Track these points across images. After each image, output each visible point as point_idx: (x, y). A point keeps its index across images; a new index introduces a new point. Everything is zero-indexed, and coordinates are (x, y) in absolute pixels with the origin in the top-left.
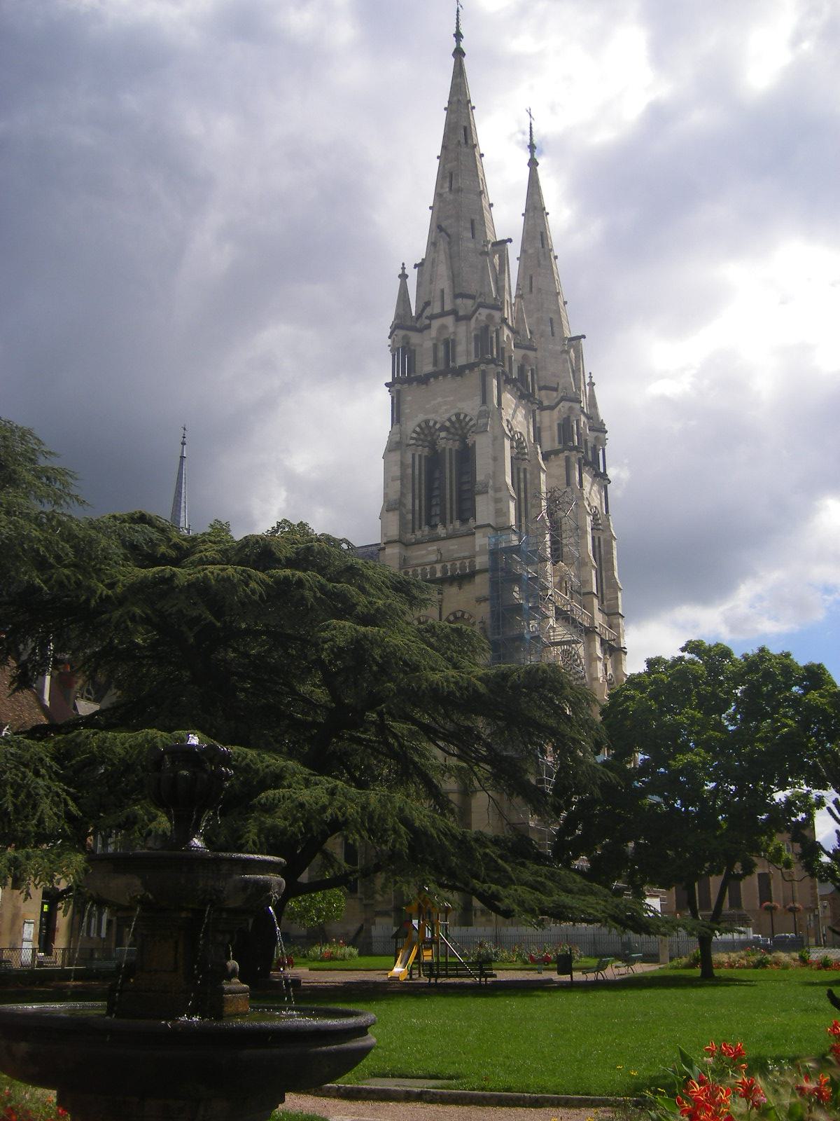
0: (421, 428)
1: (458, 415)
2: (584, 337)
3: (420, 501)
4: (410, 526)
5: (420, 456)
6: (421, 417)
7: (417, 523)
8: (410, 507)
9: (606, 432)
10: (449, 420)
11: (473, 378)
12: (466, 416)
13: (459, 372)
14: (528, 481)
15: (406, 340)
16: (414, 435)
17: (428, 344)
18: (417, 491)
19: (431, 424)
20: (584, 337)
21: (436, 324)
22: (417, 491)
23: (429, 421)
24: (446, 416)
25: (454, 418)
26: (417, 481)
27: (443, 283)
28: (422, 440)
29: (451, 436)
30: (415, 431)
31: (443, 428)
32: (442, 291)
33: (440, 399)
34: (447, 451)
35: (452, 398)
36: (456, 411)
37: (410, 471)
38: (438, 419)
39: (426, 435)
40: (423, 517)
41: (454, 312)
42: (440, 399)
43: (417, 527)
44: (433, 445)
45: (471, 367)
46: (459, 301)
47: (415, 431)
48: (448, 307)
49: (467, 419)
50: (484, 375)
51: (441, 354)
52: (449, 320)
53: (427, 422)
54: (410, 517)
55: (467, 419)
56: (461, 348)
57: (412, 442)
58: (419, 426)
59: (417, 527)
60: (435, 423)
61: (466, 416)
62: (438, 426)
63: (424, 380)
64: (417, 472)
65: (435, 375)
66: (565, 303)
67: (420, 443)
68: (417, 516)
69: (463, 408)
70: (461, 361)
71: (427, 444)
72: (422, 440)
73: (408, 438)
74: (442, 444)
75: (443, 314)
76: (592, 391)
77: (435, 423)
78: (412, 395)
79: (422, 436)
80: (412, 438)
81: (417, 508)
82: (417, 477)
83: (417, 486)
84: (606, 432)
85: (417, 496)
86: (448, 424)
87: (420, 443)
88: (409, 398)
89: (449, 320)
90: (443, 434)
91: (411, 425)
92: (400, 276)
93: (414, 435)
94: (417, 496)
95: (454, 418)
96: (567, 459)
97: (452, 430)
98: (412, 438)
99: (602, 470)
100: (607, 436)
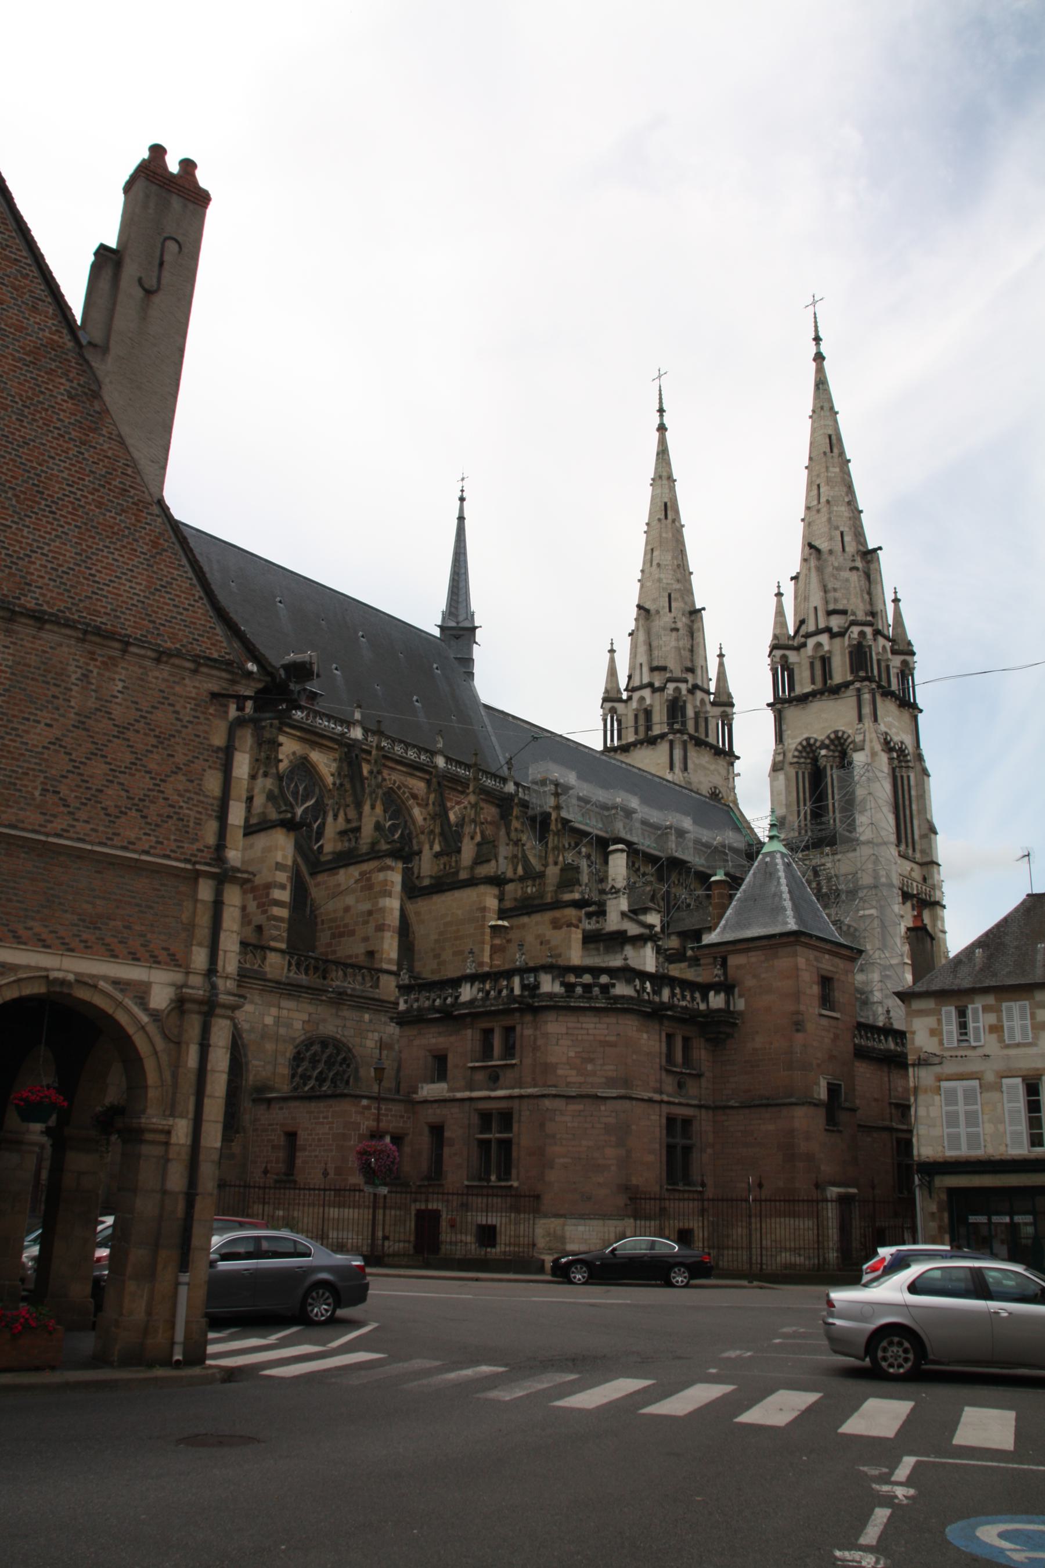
13: (835, 691)
15: (784, 657)
19: (812, 741)
21: (811, 642)
27: (816, 599)
29: (831, 753)
31: (823, 746)
32: (816, 608)
48: (821, 625)
51: (818, 672)
52: (824, 638)
62: (818, 744)
63: (804, 699)
65: (813, 694)
67: (802, 760)
75: (818, 632)
78: (792, 713)
79: (804, 754)
86: (827, 742)
87: (802, 760)
89: (824, 638)
90: (823, 752)
91: (792, 743)
92: (776, 595)
97: (832, 747)
98: (794, 757)
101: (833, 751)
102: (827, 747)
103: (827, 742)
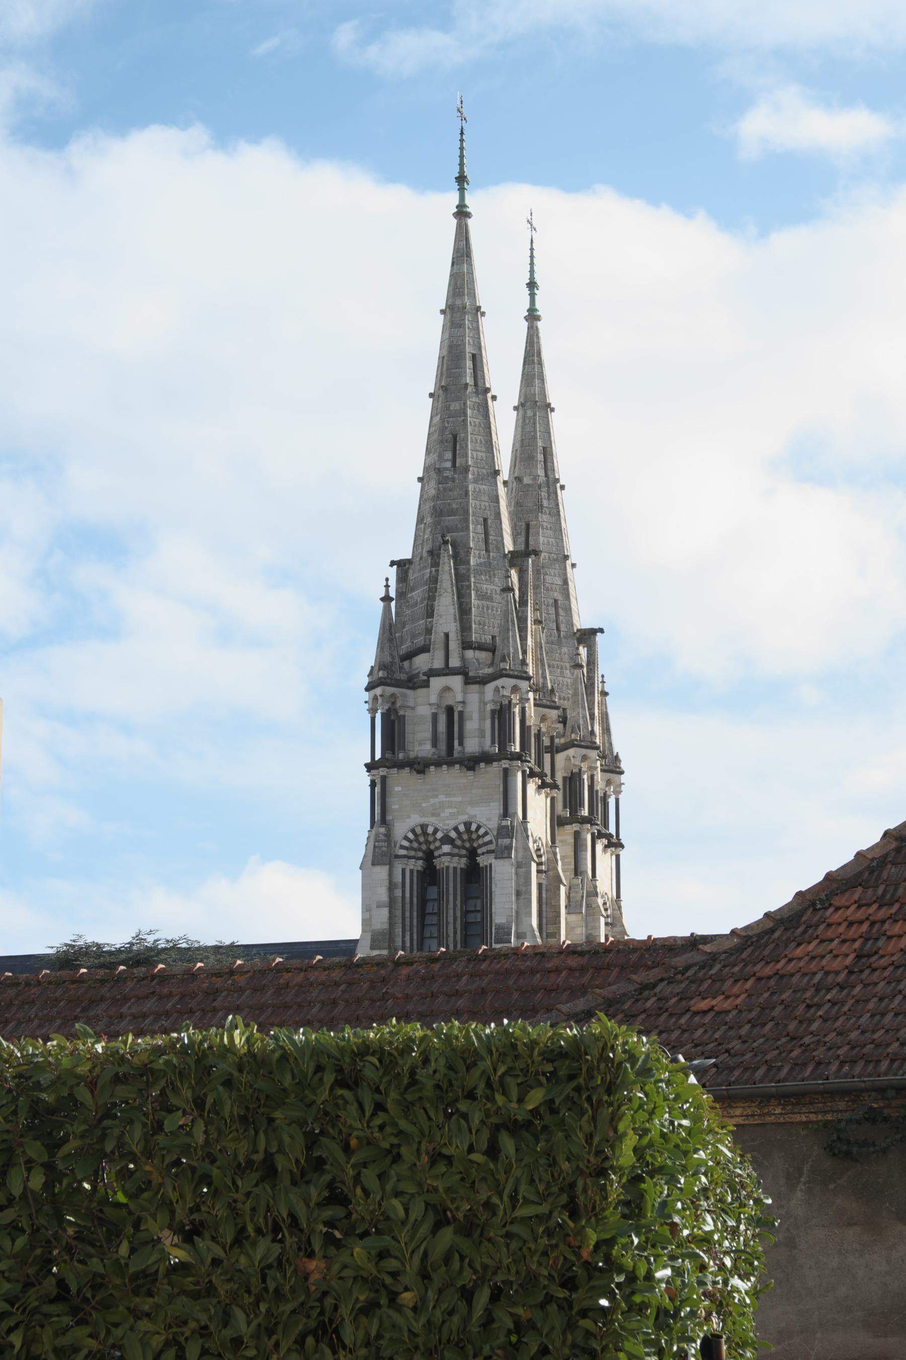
1: (468, 825)
2: (601, 631)
3: (411, 934)
5: (412, 871)
6: (415, 820)
9: (622, 773)
10: (456, 829)
11: (491, 773)
12: (479, 827)
13: (472, 763)
14: (544, 901)
16: (406, 843)
17: (424, 711)
19: (430, 830)
20: (601, 631)
21: (437, 683)
23: (427, 826)
24: (452, 823)
25: (462, 828)
26: (408, 907)
29: (456, 851)
30: (406, 838)
31: (447, 840)
32: (447, 635)
33: (442, 798)
34: (451, 871)
35: (459, 799)
36: (465, 818)
37: (398, 893)
38: (440, 825)
39: (420, 844)
41: (463, 671)
42: (442, 798)
44: (429, 856)
45: (486, 758)
46: (470, 654)
47: (406, 838)
48: (455, 662)
49: (481, 832)
50: (506, 774)
51: (442, 727)
52: (456, 682)
53: (424, 827)
55: (481, 832)
56: (471, 726)
57: (403, 852)
58: (413, 831)
60: (436, 831)
61: (479, 827)
62: (439, 835)
63: (420, 766)
64: (408, 895)
66: (573, 565)
67: (412, 853)
69: (475, 816)
70: (472, 746)
71: (420, 854)
73: (398, 846)
74: (442, 863)
75: (447, 671)
76: (603, 704)
77: (436, 831)
79: (415, 845)
80: (402, 847)
83: (408, 914)
84: (622, 773)
85: (408, 928)
86: (453, 835)
87: (412, 853)
88: (398, 789)
89: (456, 682)
90: (446, 848)
92: (382, 599)
93: (406, 843)
94: (408, 928)
95: (462, 828)
96: (577, 835)
97: (459, 843)
98: (402, 847)
99: (612, 830)
100: (623, 778)
102: (451, 841)
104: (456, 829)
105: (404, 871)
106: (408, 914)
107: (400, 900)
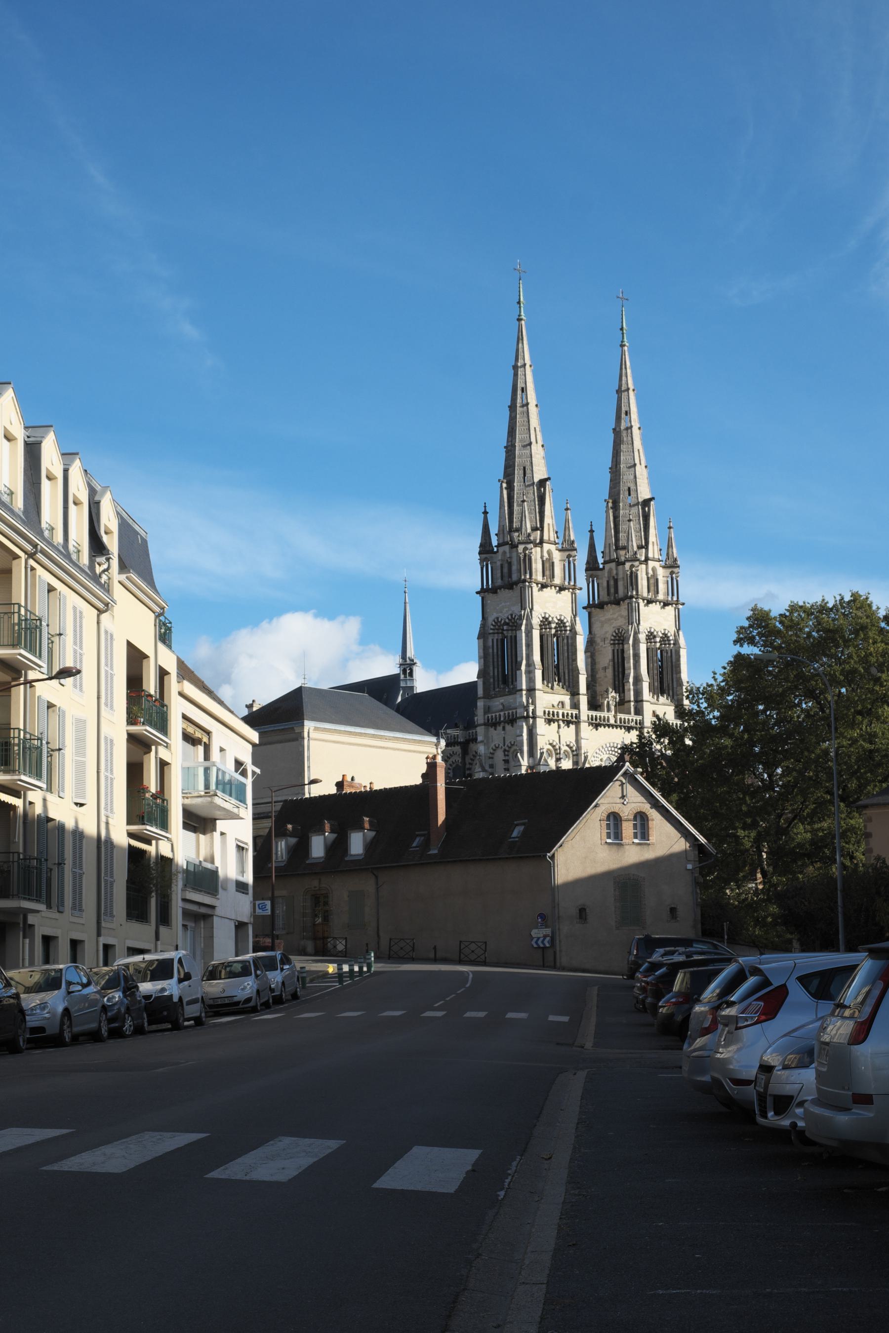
0: (495, 623)
1: (512, 615)
4: (492, 686)
6: (495, 615)
7: (496, 683)
8: (492, 674)
16: (492, 627)
18: (496, 663)
22: (496, 663)
24: (506, 615)
25: (510, 617)
26: (495, 657)
28: (497, 629)
29: (510, 628)
30: (492, 625)
33: (503, 604)
36: (510, 612)
37: (491, 650)
40: (500, 679)
42: (503, 604)
43: (496, 686)
47: (492, 625)
53: (498, 618)
54: (492, 680)
57: (491, 631)
59: (496, 686)
62: (503, 622)
67: (496, 631)
68: (496, 679)
72: (497, 629)
79: (497, 627)
80: (491, 629)
81: (496, 674)
82: (495, 653)
83: (495, 660)
86: (507, 621)
87: (496, 631)
91: (490, 620)
93: (492, 627)
98: (491, 629)
101: (512, 626)
102: (507, 624)
103: (507, 621)
104: (508, 618)
105: (493, 640)
106: (495, 660)
107: (491, 654)
